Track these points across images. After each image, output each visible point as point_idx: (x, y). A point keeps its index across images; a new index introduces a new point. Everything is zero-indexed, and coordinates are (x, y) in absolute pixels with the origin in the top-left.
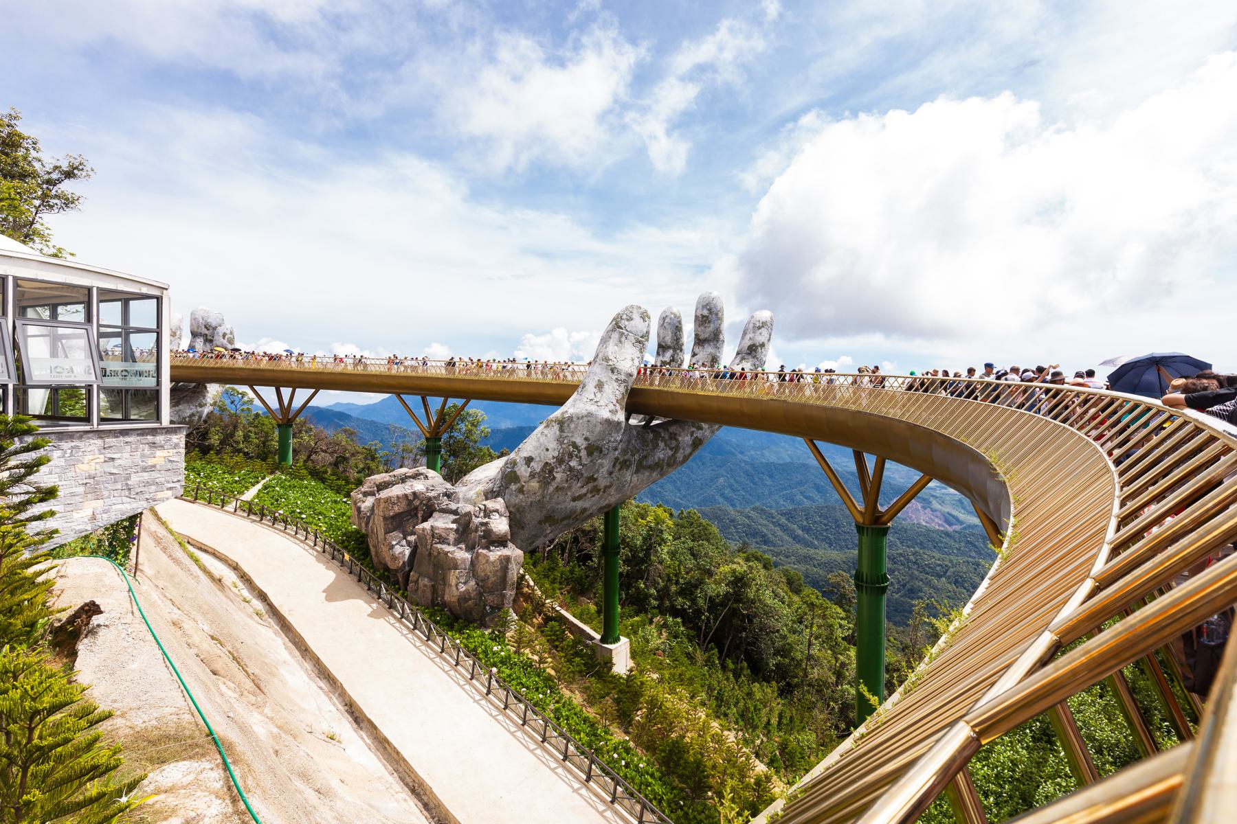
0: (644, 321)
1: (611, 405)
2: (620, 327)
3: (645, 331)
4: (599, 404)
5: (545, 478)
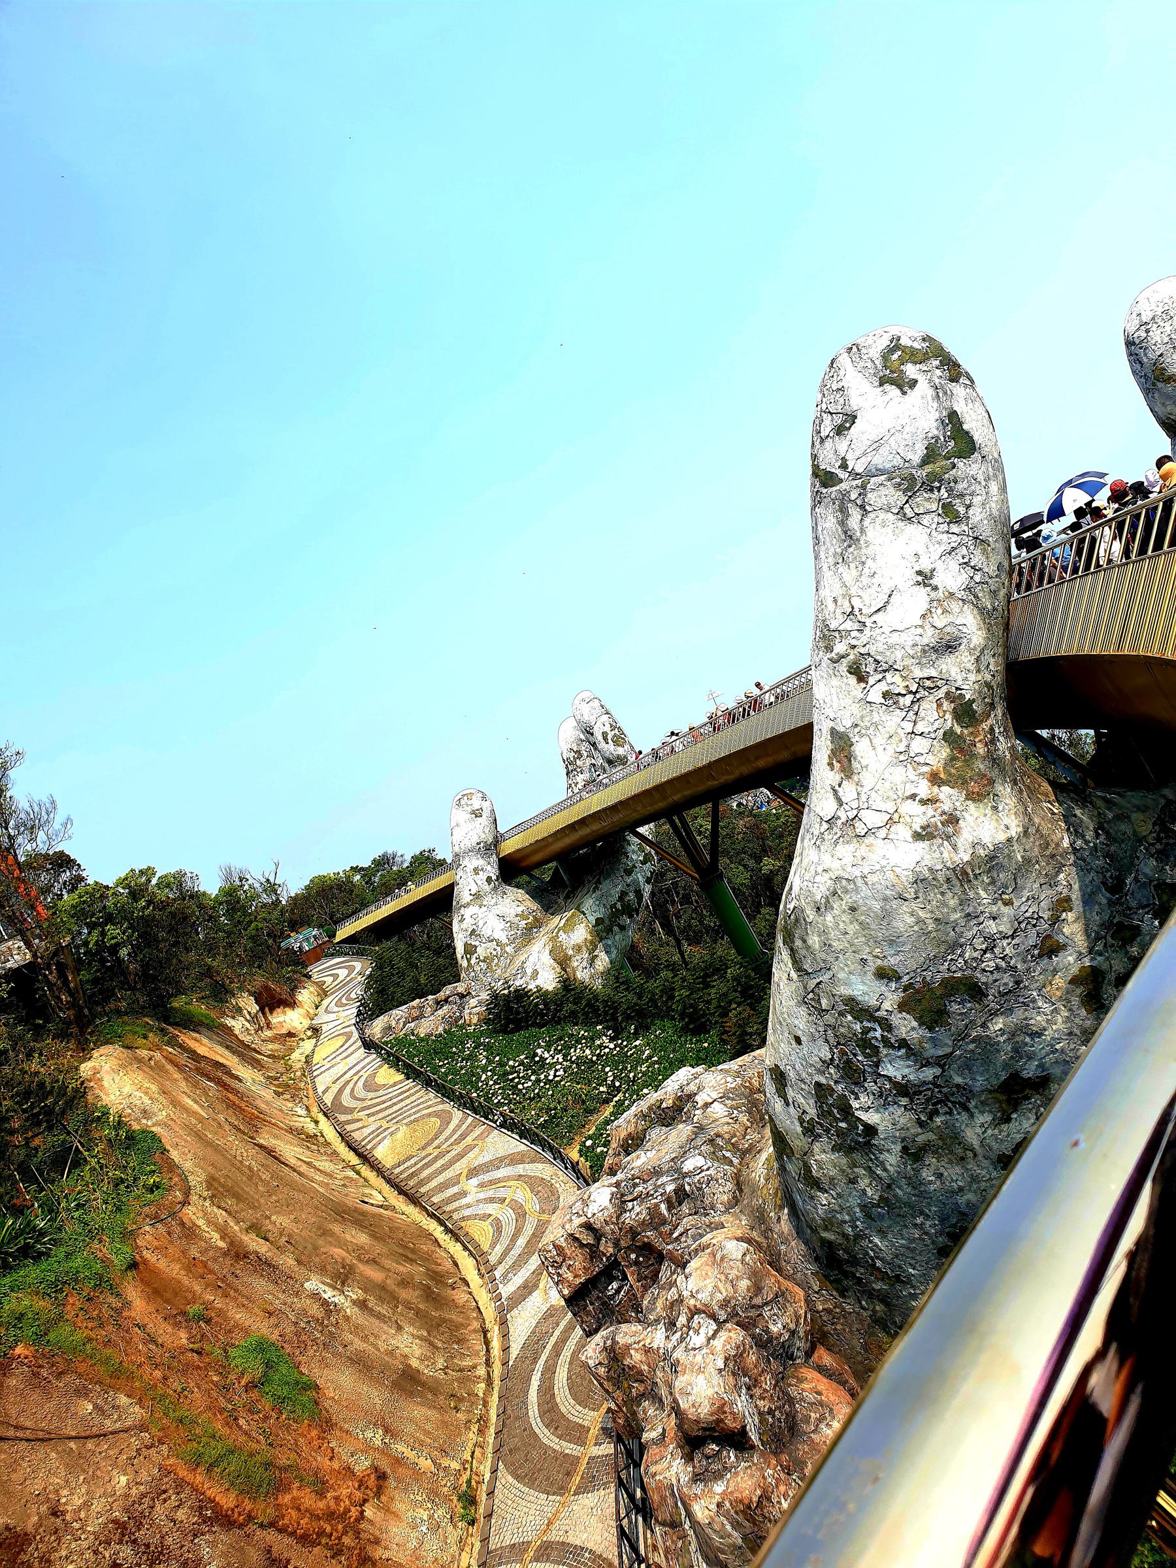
0: (905, 385)
4: (860, 829)
5: (840, 1133)
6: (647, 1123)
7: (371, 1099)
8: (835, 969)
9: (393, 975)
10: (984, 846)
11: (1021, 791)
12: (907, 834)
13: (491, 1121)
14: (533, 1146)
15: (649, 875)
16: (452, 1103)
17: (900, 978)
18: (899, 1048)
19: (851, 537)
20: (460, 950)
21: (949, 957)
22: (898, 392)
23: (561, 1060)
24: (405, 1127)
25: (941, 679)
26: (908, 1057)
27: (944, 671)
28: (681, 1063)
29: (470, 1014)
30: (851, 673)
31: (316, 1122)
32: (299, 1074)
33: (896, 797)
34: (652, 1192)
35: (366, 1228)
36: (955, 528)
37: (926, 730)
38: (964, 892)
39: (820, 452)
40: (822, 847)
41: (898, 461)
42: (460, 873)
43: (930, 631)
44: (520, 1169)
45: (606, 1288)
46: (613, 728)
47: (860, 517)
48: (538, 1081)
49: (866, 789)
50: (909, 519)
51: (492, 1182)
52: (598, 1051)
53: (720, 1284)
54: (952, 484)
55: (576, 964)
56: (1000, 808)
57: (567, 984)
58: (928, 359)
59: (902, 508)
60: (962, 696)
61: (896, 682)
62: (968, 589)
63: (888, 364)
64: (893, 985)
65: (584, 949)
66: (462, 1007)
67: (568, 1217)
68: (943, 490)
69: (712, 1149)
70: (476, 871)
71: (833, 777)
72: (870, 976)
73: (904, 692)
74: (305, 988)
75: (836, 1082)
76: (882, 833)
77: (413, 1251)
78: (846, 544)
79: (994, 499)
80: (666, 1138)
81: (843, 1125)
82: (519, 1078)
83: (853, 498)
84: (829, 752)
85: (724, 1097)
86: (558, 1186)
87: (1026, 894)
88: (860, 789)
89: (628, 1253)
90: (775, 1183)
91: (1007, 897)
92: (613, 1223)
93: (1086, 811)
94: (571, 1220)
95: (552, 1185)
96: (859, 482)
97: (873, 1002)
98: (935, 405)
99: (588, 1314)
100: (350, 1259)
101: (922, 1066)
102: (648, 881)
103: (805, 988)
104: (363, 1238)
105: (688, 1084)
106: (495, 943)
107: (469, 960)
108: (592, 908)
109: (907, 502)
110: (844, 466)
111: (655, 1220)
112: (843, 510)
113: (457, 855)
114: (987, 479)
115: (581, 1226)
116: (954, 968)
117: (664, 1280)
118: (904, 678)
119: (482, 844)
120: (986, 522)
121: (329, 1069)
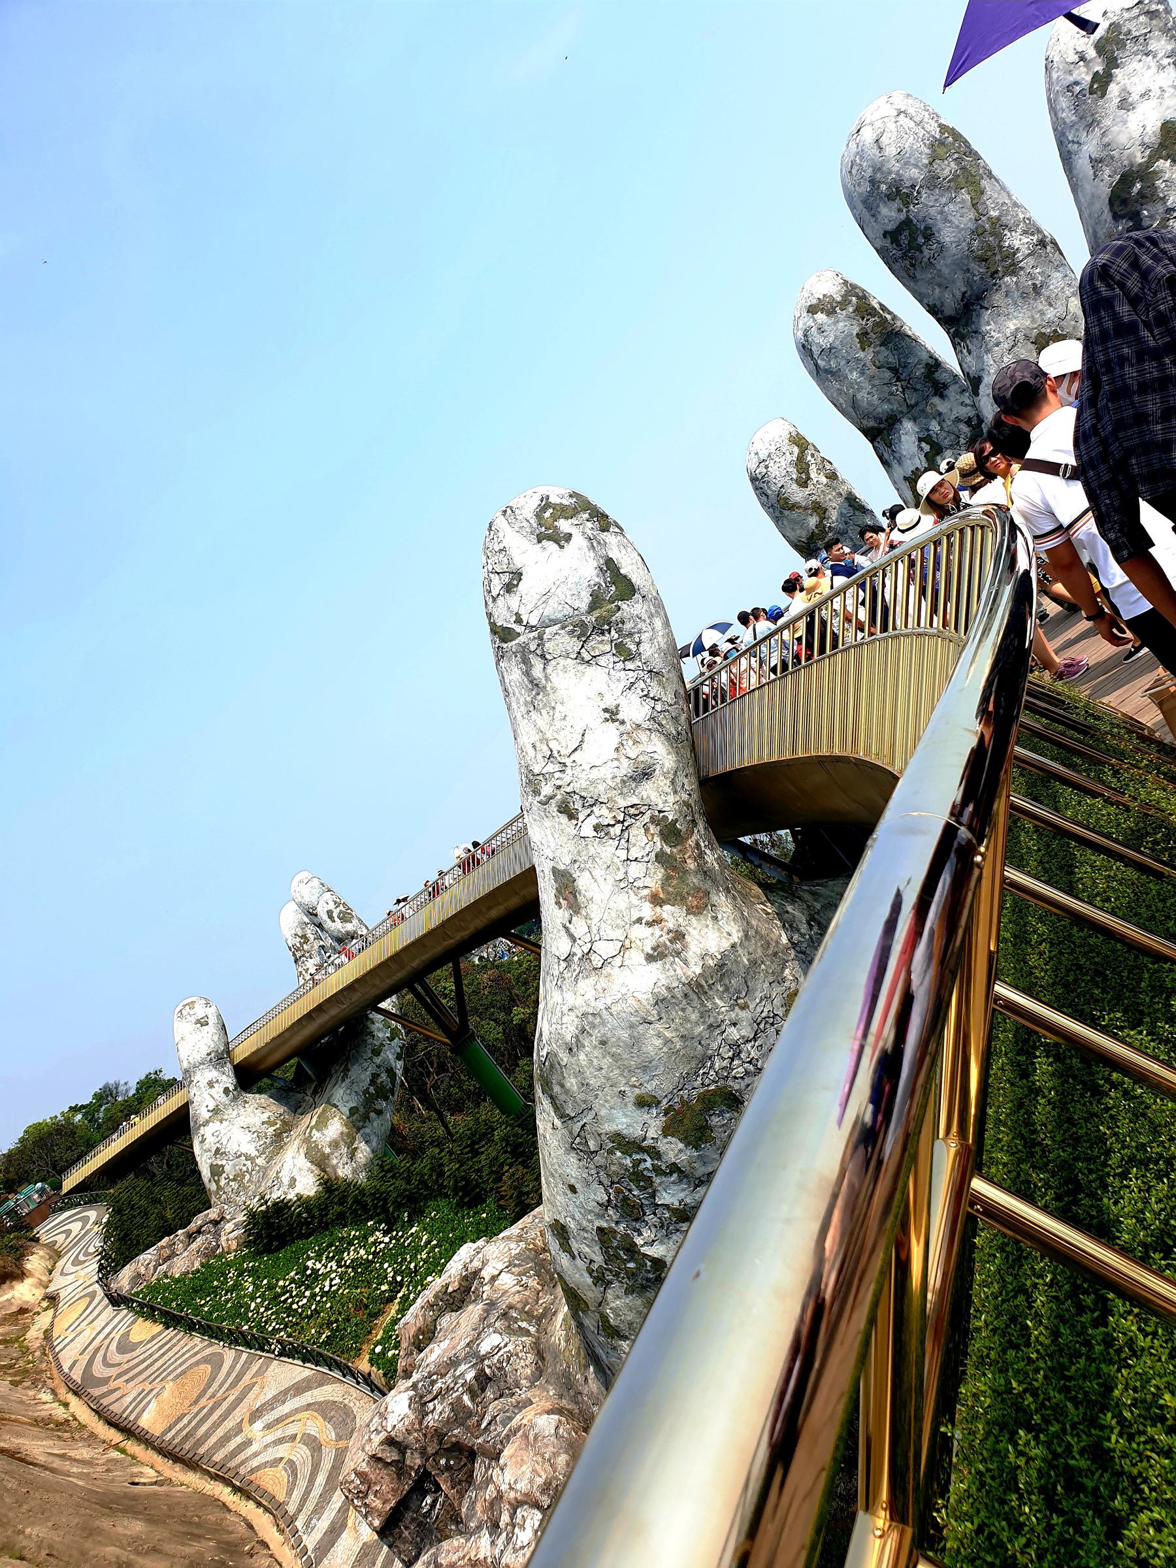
5: (631, 1275)
6: (436, 1312)
7: (128, 1362)
8: (596, 1107)
9: (134, 1217)
10: (712, 957)
11: (734, 898)
12: (641, 958)
13: (268, 1352)
14: (318, 1368)
15: (398, 1050)
16: (222, 1343)
17: (659, 1102)
18: (671, 1174)
19: (537, 685)
20: (206, 1173)
21: (701, 1072)
22: (556, 546)
23: (334, 1268)
24: (171, 1384)
26: (681, 1181)
27: (645, 797)
28: (462, 1241)
29: (228, 1240)
30: (561, 812)
31: (66, 1405)
32: (38, 1354)
33: (623, 923)
34: (452, 1385)
35: (140, 1513)
36: (629, 665)
37: (639, 855)
38: (703, 1004)
39: (494, 610)
40: (564, 987)
41: (568, 611)
42: (193, 1090)
43: (625, 763)
44: (308, 1397)
45: (420, 1507)
46: (337, 904)
47: (542, 666)
48: (314, 1295)
49: (595, 921)
50: (588, 662)
51: (278, 1421)
52: (373, 1249)
53: (538, 1468)
54: (620, 625)
55: (335, 1162)
56: (720, 917)
57: (329, 1185)
58: (579, 512)
61: (603, 814)
62: (652, 719)
63: (542, 522)
64: (654, 1111)
65: (342, 1144)
66: (217, 1236)
67: (366, 1437)
68: (613, 632)
69: (507, 1324)
70: (211, 1084)
72: (631, 1107)
73: (612, 822)
74: (33, 1254)
75: (617, 1223)
76: (617, 961)
77: (198, 1525)
78: (534, 693)
79: (660, 633)
80: (458, 1323)
81: (631, 1265)
82: (291, 1296)
83: (532, 650)
84: (554, 891)
85: (511, 1264)
86: (352, 1405)
87: (759, 995)
88: (589, 922)
89: (437, 1460)
90: (576, 1342)
91: (742, 1001)
92: (416, 1431)
93: (796, 905)
94: (370, 1440)
95: (345, 1405)
96: (535, 634)
97: (638, 1132)
98: (592, 554)
99: (405, 1541)
100: (125, 1555)
101: (696, 1186)
102: (399, 1057)
103: (571, 1133)
104: (137, 1527)
105: (471, 1261)
107: (217, 1182)
108: (343, 1097)
109: (583, 646)
110: (519, 621)
111: (460, 1415)
112: (526, 661)
113: (186, 1071)
114: (651, 616)
115: (382, 1443)
116: (707, 1082)
117: (479, 1479)
118: (610, 810)
119: (213, 1055)
120: (656, 655)
121: (72, 1340)
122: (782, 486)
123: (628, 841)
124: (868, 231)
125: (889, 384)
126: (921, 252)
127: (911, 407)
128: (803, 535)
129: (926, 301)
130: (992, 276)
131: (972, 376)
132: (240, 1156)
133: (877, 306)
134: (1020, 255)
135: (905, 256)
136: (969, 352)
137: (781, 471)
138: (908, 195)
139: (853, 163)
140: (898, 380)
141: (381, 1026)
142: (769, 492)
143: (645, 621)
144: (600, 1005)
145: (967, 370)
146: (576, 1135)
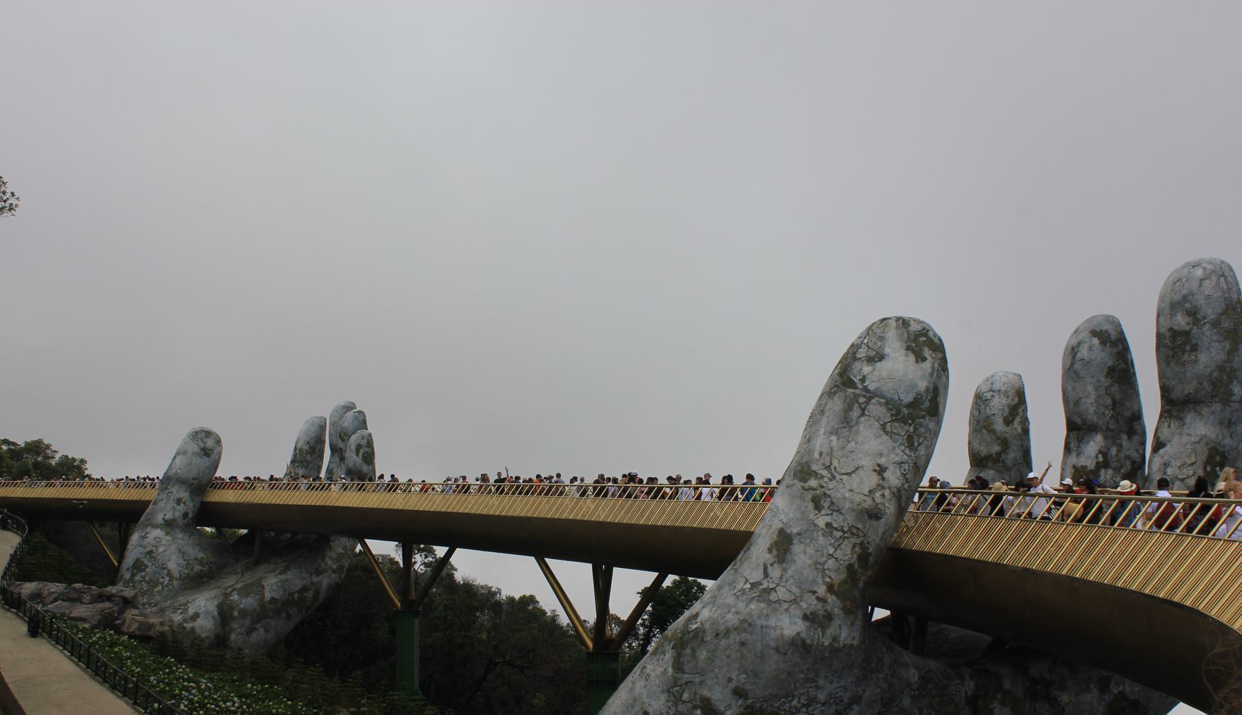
0: (920, 358)
1: (812, 600)
2: (851, 384)
3: (922, 385)
12: (799, 613)
19: (848, 422)
25: (863, 532)
36: (907, 451)
37: (840, 557)
43: (869, 500)
47: (859, 415)
54: (918, 426)
56: (855, 624)
57: (221, 640)
59: (885, 423)
60: (868, 548)
71: (769, 558)
72: (729, 690)
76: (786, 606)
78: (842, 425)
88: (784, 572)
96: (868, 395)
97: (722, 708)
106: (166, 572)
107: (133, 575)
109: (890, 422)
110: (863, 380)
116: (782, 707)
119: (196, 482)
120: (924, 457)
122: (993, 415)
123: (839, 545)
124: (1162, 319)
125: (1106, 407)
126: (1184, 354)
127: (1108, 429)
128: (984, 450)
129: (1164, 381)
130: (1212, 397)
131: (1160, 440)
132: (165, 569)
133: (1130, 359)
134: (1234, 398)
135: (1172, 349)
136: (1169, 426)
137: (999, 404)
138: (1199, 320)
139: (1179, 280)
140: (1113, 409)
141: (334, 556)
142: (983, 411)
143: (931, 434)
144: (759, 623)
145: (1159, 434)
146: (679, 684)
